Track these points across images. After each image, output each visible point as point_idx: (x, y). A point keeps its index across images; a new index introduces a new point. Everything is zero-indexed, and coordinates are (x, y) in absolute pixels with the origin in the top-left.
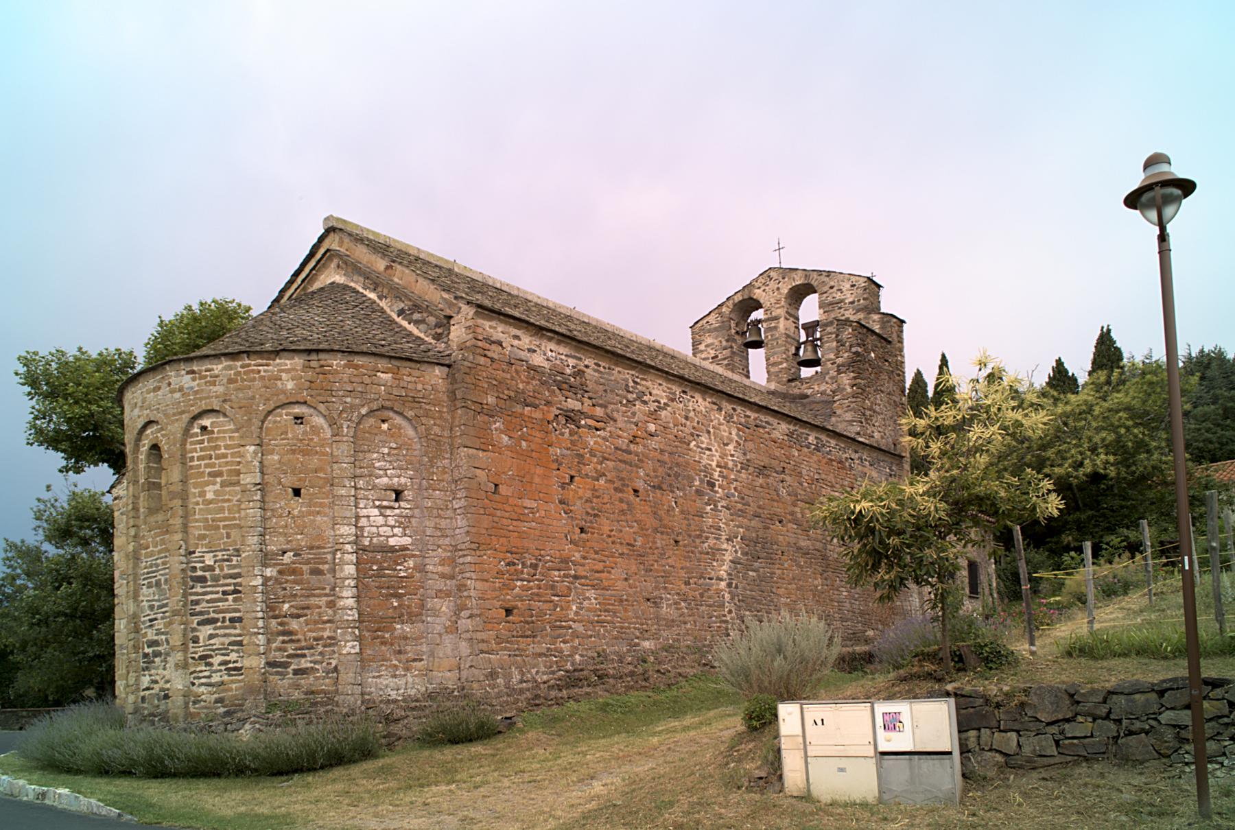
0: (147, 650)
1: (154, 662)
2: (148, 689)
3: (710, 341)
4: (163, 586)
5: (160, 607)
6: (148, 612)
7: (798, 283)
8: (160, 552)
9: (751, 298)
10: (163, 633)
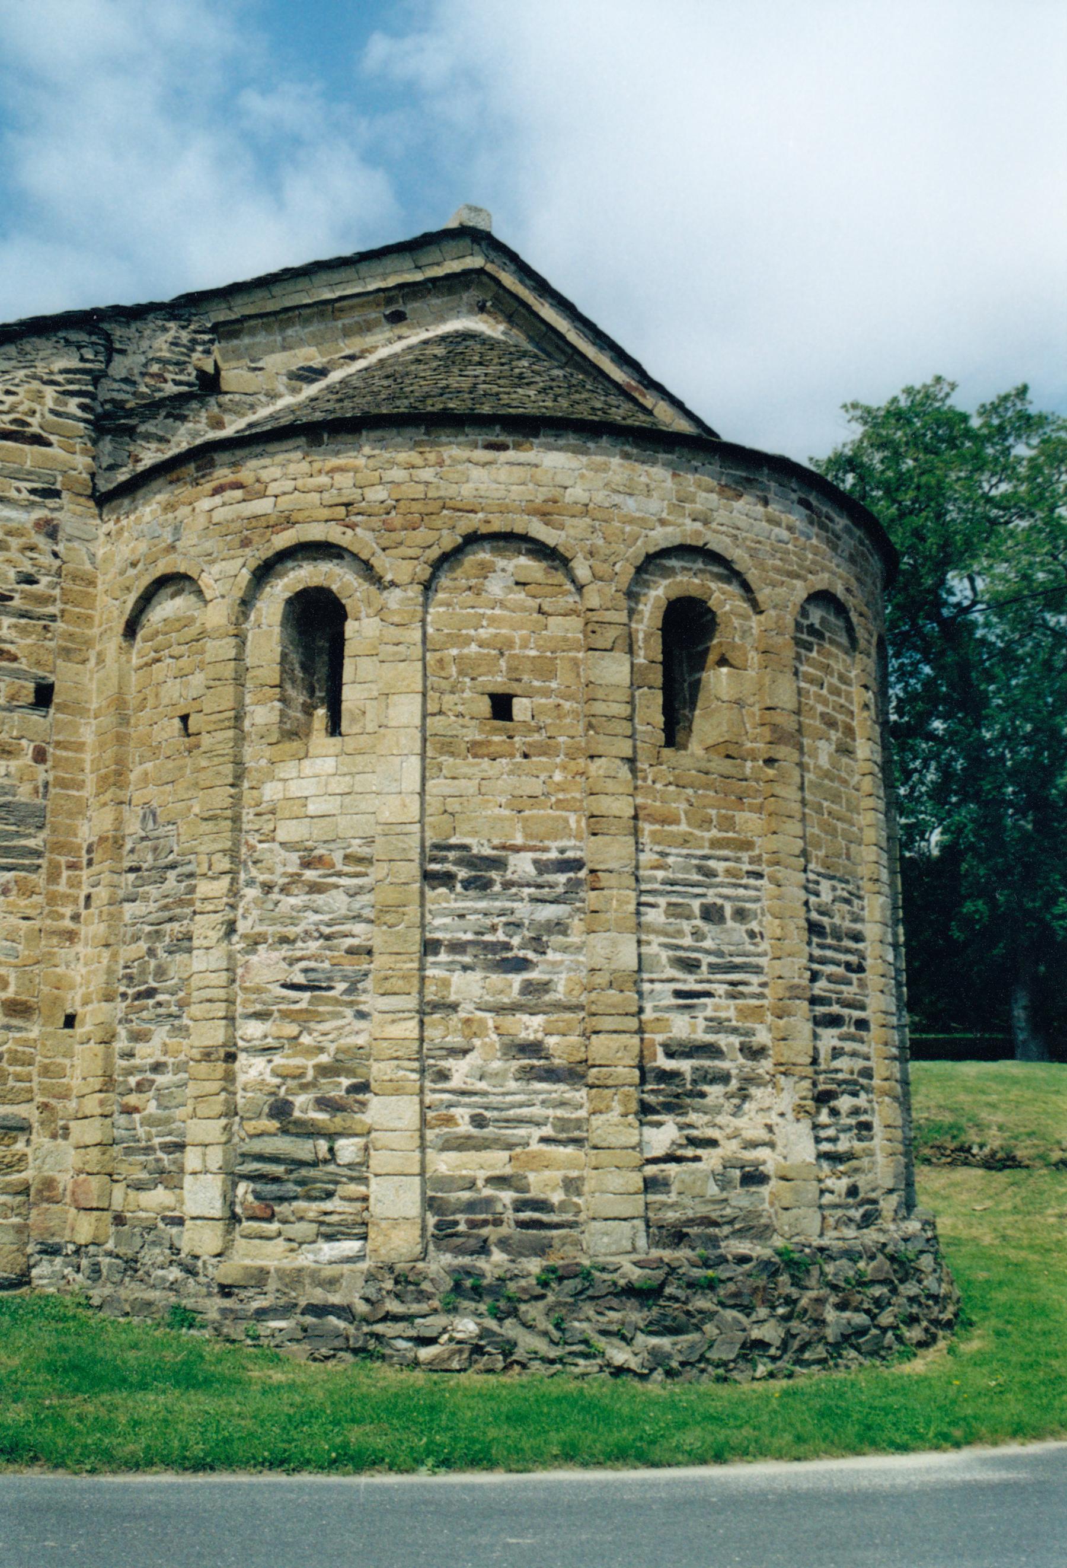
1: (703, 1095)
2: (671, 1158)
4: (730, 923)
5: (713, 968)
8: (715, 844)
10: (735, 1031)
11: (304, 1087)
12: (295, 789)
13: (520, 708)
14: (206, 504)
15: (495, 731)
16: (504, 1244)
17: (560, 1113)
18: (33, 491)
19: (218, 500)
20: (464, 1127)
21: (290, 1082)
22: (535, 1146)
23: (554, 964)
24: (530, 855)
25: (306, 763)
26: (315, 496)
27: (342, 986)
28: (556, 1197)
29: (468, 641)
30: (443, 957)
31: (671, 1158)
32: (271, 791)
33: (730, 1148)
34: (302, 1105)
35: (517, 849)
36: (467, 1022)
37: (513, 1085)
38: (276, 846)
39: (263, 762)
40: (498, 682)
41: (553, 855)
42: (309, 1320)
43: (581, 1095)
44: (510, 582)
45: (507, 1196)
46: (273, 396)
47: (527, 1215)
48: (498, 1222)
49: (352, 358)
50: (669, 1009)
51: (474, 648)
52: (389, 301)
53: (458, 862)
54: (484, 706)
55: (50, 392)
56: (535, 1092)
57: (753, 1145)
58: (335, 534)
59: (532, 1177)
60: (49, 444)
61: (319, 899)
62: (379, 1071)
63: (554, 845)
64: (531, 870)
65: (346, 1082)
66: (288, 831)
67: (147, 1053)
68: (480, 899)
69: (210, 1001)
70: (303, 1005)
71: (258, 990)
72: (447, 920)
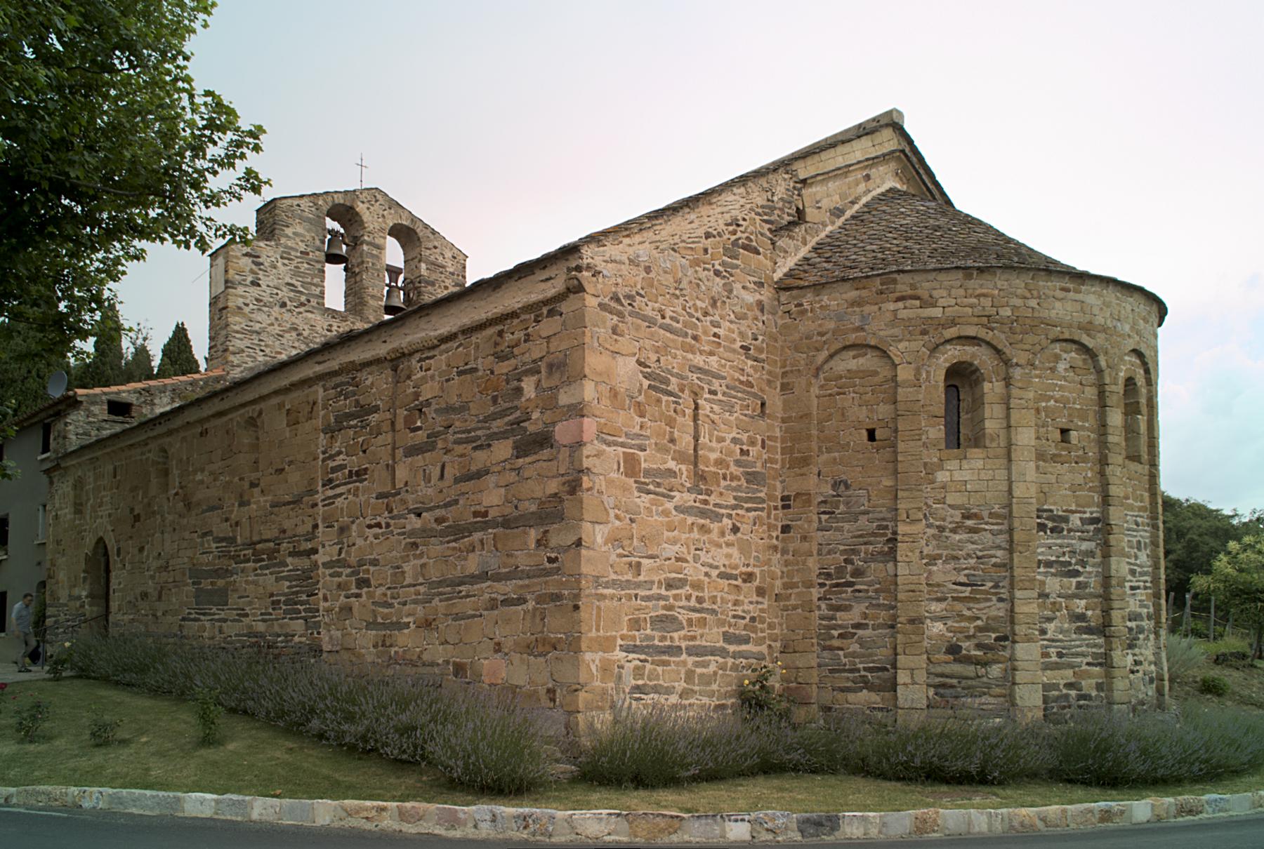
3: (299, 229)
7: (404, 223)
9: (352, 208)
11: (968, 638)
12: (958, 476)
14: (892, 306)
15: (1063, 449)
17: (1094, 650)
19: (900, 304)
20: (1054, 659)
22: (1084, 667)
23: (1090, 573)
24: (1078, 515)
25: (964, 462)
26: (969, 310)
27: (991, 584)
28: (1094, 693)
30: (1042, 570)
32: (942, 477)
34: (968, 647)
35: (1073, 512)
36: (1054, 604)
37: (1074, 636)
39: (935, 460)
40: (1063, 422)
43: (1101, 641)
44: (1068, 366)
45: (1073, 693)
47: (1082, 702)
48: (1070, 707)
51: (1052, 402)
54: (1058, 436)
58: (982, 333)
60: (759, 253)
61: (976, 537)
63: (1088, 510)
64: (1079, 523)
65: (994, 636)
68: (1058, 538)
69: (913, 591)
70: (967, 594)
71: (938, 585)
72: (1043, 549)
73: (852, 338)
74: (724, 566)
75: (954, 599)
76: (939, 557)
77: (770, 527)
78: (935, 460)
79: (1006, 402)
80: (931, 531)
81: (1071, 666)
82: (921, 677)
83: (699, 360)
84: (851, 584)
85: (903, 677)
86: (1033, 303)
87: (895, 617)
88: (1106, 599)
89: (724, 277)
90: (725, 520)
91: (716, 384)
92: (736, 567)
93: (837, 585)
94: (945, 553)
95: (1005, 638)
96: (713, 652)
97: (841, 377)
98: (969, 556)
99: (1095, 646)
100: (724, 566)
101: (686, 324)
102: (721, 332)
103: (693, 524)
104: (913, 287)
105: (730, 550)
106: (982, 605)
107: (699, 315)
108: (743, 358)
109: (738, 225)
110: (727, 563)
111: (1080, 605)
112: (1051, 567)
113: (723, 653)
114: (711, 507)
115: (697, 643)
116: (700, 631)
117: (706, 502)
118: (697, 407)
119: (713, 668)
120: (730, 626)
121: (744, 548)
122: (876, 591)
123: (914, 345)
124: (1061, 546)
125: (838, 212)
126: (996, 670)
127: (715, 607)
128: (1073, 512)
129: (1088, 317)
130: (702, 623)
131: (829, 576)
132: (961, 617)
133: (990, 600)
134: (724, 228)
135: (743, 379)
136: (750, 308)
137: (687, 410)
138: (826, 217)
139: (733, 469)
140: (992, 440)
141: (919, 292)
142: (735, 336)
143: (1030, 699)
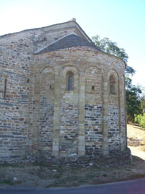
0: (110, 132)
2: (111, 143)
5: (114, 120)
6: (111, 121)
10: (116, 127)
11: (69, 134)
12: (67, 97)
13: (95, 88)
14: (55, 58)
16: (94, 153)
18: (27, 53)
21: (67, 134)
23: (99, 120)
26: (71, 59)
28: (99, 148)
29: (89, 79)
30: (87, 119)
31: (111, 143)
32: (64, 97)
33: (116, 141)
35: (95, 105)
38: (65, 104)
41: (99, 106)
42: (72, 164)
43: (102, 135)
44: (94, 72)
45: (94, 148)
46: (52, 41)
48: (93, 151)
49: (61, 37)
50: (110, 125)
51: (90, 80)
52: (65, 30)
53: (88, 107)
54: (91, 88)
55: (29, 39)
56: (97, 135)
57: (117, 141)
59: (97, 145)
60: (29, 47)
61: (71, 111)
62: (80, 133)
65: (75, 134)
66: (66, 102)
67: (44, 129)
68: (91, 111)
71: (63, 122)
73: (47, 65)
74: (13, 117)
75: (66, 125)
76: (63, 115)
77: (29, 108)
78: (63, 93)
79: (78, 79)
80: (62, 109)
81: (94, 141)
82: (58, 144)
83: (7, 69)
84: (45, 121)
85: (54, 144)
86: (85, 58)
87: (53, 129)
88: (102, 126)
89: (17, 52)
90: (14, 106)
91: (13, 75)
92: (17, 117)
93: (43, 122)
94: (64, 114)
95: (77, 135)
96: (9, 136)
97: (45, 74)
98: (70, 115)
99: (100, 137)
100: (13, 117)
101: (4, 62)
102: (15, 64)
103: (3, 107)
104: (59, 54)
105: (15, 113)
106: (71, 127)
107: (8, 60)
108: (22, 69)
109: (23, 41)
110: (14, 116)
111: (97, 127)
112: (89, 118)
113: (12, 137)
114: (10, 103)
115: (4, 134)
116: (4, 132)
117: (8, 102)
118: (6, 80)
119: (9, 140)
120: (15, 131)
121: (21, 112)
122: (50, 123)
123: (59, 67)
124: (92, 113)
125: (56, 39)
126: (75, 142)
127: (10, 126)
128: (95, 105)
129: (99, 62)
130: (6, 130)
131: (41, 119)
132: (68, 130)
133: (74, 126)
134: (18, 41)
135: (23, 74)
136: (25, 58)
137: (3, 81)
138: (53, 40)
139: (18, 94)
140: (76, 88)
141: (60, 55)
142: (20, 64)
143: (82, 149)
